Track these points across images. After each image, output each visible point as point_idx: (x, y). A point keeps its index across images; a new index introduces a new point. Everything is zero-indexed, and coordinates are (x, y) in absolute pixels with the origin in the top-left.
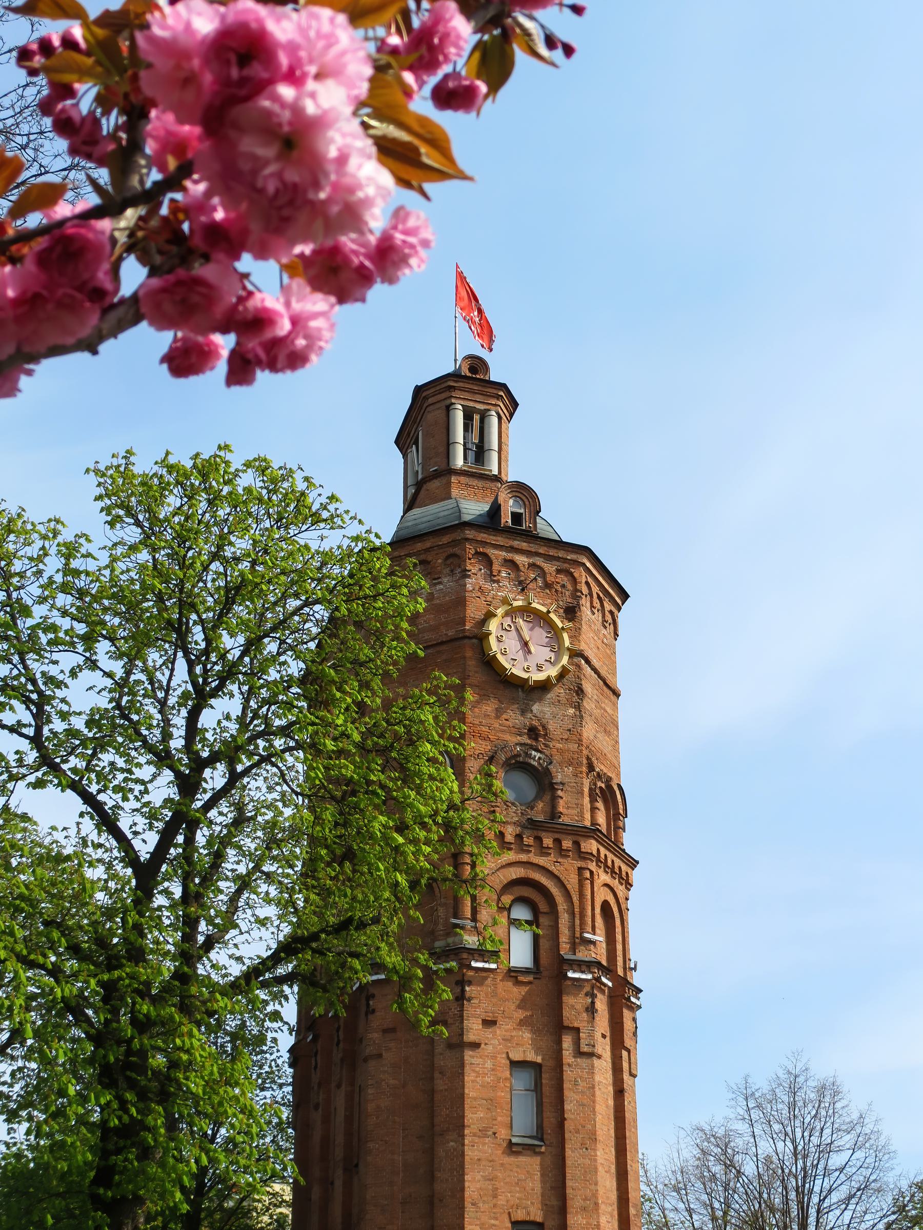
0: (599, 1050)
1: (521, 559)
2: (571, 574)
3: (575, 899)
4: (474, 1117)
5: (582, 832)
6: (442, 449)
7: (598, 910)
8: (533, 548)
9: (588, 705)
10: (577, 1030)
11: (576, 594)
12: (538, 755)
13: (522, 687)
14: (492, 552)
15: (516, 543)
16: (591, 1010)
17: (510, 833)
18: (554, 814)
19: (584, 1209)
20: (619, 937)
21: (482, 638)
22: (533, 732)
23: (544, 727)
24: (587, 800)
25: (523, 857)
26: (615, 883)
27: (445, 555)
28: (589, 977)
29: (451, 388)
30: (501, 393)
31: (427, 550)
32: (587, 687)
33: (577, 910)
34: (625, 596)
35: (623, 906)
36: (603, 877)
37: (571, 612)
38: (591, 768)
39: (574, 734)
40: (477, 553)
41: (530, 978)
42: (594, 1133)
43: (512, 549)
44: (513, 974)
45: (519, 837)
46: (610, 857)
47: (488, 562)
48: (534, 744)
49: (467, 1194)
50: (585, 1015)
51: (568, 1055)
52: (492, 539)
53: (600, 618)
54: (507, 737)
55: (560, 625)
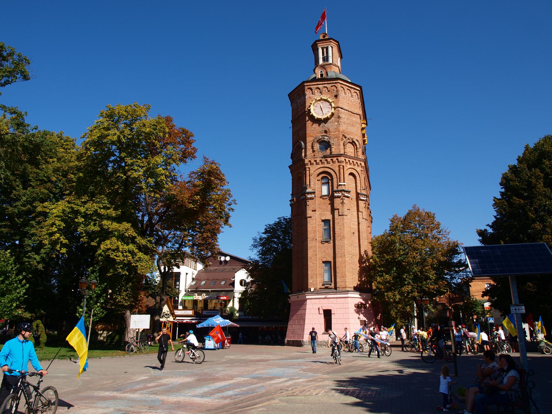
3: (338, 174)
4: (310, 236)
10: (338, 209)
11: (337, 91)
14: (312, 87)
15: (318, 83)
16: (343, 203)
18: (331, 153)
21: (309, 110)
22: (326, 132)
24: (342, 146)
25: (323, 166)
34: (360, 87)
35: (360, 173)
36: (349, 166)
37: (336, 96)
38: (345, 137)
39: (337, 129)
47: (311, 89)
49: (309, 255)
53: (350, 95)
54: (318, 135)
55: (331, 101)
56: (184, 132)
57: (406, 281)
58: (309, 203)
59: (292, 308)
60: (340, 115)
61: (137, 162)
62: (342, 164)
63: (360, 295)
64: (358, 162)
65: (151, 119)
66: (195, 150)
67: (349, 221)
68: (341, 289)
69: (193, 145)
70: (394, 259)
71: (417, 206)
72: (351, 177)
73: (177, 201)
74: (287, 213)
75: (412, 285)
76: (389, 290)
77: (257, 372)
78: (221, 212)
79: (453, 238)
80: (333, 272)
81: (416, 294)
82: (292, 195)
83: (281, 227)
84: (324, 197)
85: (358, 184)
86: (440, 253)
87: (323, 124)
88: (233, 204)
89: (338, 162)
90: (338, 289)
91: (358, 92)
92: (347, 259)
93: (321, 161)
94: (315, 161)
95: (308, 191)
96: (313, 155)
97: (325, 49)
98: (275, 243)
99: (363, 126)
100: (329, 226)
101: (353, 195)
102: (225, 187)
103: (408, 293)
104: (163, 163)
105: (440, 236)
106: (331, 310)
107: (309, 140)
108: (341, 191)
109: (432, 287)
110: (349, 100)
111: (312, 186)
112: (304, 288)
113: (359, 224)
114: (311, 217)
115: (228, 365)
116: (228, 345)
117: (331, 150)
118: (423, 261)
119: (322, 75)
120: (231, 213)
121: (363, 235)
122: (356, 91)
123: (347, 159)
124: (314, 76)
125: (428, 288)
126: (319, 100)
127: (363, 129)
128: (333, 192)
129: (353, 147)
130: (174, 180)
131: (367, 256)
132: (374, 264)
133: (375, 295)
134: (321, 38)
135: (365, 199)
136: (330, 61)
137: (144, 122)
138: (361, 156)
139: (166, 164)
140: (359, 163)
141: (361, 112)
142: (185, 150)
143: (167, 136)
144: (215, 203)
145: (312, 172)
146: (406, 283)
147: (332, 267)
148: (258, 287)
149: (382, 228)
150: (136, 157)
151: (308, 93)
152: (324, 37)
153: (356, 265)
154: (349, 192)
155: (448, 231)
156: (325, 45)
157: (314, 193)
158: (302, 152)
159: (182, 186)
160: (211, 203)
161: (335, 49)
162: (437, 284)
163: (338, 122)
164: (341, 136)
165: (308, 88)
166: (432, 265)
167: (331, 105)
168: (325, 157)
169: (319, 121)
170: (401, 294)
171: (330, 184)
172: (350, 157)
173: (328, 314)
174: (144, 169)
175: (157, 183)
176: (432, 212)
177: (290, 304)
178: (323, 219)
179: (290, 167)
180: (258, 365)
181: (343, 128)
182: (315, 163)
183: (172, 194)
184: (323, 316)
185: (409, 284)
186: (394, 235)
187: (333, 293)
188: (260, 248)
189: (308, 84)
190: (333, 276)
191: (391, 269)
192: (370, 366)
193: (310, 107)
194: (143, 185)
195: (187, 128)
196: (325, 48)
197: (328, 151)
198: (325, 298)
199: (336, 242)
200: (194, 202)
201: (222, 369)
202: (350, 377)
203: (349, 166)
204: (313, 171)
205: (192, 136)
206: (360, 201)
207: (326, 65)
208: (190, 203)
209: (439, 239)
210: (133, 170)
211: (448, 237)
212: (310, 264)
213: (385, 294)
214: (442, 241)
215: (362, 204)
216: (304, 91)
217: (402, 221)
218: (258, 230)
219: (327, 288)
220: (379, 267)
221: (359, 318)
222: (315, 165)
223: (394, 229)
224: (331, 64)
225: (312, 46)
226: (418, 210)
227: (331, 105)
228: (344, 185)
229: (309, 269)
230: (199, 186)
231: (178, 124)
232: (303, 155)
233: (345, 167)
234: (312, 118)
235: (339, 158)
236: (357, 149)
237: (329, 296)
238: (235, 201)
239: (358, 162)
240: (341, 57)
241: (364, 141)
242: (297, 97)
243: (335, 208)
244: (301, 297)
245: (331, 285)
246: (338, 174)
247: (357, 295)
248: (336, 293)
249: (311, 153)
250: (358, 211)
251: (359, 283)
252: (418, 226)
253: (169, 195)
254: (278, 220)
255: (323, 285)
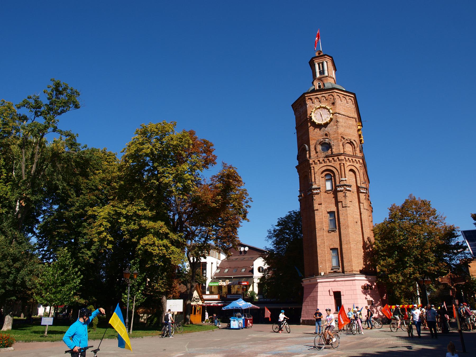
1: (318, 96)
3: (339, 171)
4: (318, 226)
14: (311, 97)
15: (317, 93)
16: (345, 196)
18: (332, 153)
19: (347, 243)
21: (311, 118)
22: (326, 135)
24: (341, 147)
25: (325, 164)
33: (340, 173)
34: (354, 94)
35: (359, 169)
36: (349, 164)
37: (333, 104)
38: (344, 139)
39: (336, 132)
42: (348, 225)
44: (326, 192)
47: (311, 99)
50: (343, 198)
51: (340, 208)
54: (320, 138)
55: (329, 108)
56: (205, 142)
57: (407, 263)
58: (315, 197)
59: (305, 291)
60: (338, 120)
61: (167, 170)
62: (343, 162)
63: (366, 277)
64: (356, 159)
65: (177, 133)
66: (215, 157)
67: (351, 212)
68: (348, 273)
69: (213, 153)
70: (395, 244)
71: (413, 196)
72: (351, 173)
73: (202, 201)
74: (296, 207)
75: (414, 267)
76: (392, 272)
77: (278, 349)
78: (239, 209)
79: (449, 222)
80: (340, 257)
81: (418, 275)
82: (300, 191)
83: (292, 220)
84: (328, 192)
85: (358, 179)
86: (438, 237)
87: (323, 129)
88: (250, 202)
89: (339, 160)
90: (345, 273)
91: (352, 99)
92: (352, 246)
93: (324, 160)
94: (319, 161)
95: (313, 187)
96: (316, 155)
97: (321, 64)
98: (287, 233)
99: (359, 127)
100: (334, 216)
101: (354, 189)
102: (242, 188)
103: (410, 275)
104: (189, 170)
105: (437, 222)
106: (340, 292)
107: (312, 143)
108: (343, 186)
109: (432, 268)
110: (345, 106)
111: (317, 182)
112: (315, 273)
113: (361, 214)
114: (317, 210)
115: (251, 342)
116: (251, 325)
117: (331, 150)
118: (422, 246)
119: (319, 87)
120: (248, 210)
121: (366, 224)
122: (350, 98)
123: (347, 158)
124: (313, 88)
125: (429, 269)
126: (319, 108)
127: (359, 130)
128: (336, 187)
129: (351, 146)
130: (198, 183)
131: (370, 242)
132: (377, 249)
133: (380, 277)
134: (317, 55)
135: (365, 191)
136: (326, 74)
137: (171, 135)
138: (359, 154)
139: (192, 170)
141: (356, 116)
142: (207, 158)
143: (191, 147)
144: (234, 201)
145: (316, 170)
146: (408, 265)
147: (339, 253)
148: (274, 273)
149: (382, 216)
150: (166, 166)
151: (309, 103)
152: (319, 54)
153: (361, 250)
154: (350, 186)
155: (443, 217)
156: (320, 60)
157: (319, 188)
158: (306, 154)
159: (206, 189)
160: (231, 202)
161: (330, 63)
162: (438, 265)
163: (337, 126)
164: (340, 138)
165: (309, 99)
166: (431, 248)
167: (329, 111)
168: (327, 157)
169: (320, 126)
170: (404, 275)
171: (333, 180)
172: (349, 156)
173: (337, 295)
174: (174, 175)
175: (184, 187)
176: (428, 200)
177: (303, 287)
178: (329, 211)
179: (297, 167)
180: (278, 342)
181: (341, 130)
182: (318, 162)
183: (197, 196)
184: (333, 297)
185: (410, 266)
186: (394, 222)
187: (341, 276)
188: (275, 238)
189: (308, 95)
190: (340, 262)
191: (393, 253)
192: (380, 342)
193: (311, 114)
194: (173, 189)
195: (207, 139)
196: (320, 63)
197: (329, 151)
198: (334, 281)
199: (342, 231)
200: (216, 201)
201: (247, 346)
202: (362, 353)
203: (349, 164)
204: (317, 170)
205: (212, 145)
206: (360, 194)
207: (323, 77)
208: (213, 202)
209: (436, 224)
210: (164, 176)
211: (445, 222)
212: (319, 251)
213: (389, 276)
214: (439, 226)
215: (362, 196)
216: (305, 101)
217: (400, 210)
218: (272, 223)
219: (335, 272)
220: (382, 251)
221: (366, 298)
222: (318, 165)
223: (393, 217)
224: (327, 76)
225: (309, 63)
226: (415, 199)
227: (329, 111)
228: (346, 180)
229: (319, 256)
230: (220, 188)
231: (200, 136)
232: (308, 156)
233: (345, 164)
234: (313, 124)
235: (339, 157)
236: (354, 148)
237: (337, 279)
238: (251, 198)
239: (356, 159)
240: (335, 70)
241: (361, 141)
242: (300, 107)
243: (339, 201)
244: (312, 281)
245: (339, 269)
246: (339, 171)
247: (363, 277)
248: (344, 276)
249: (315, 155)
250: (359, 202)
251: (364, 267)
252: (415, 213)
253: (195, 197)
254: (289, 214)
255: (332, 269)
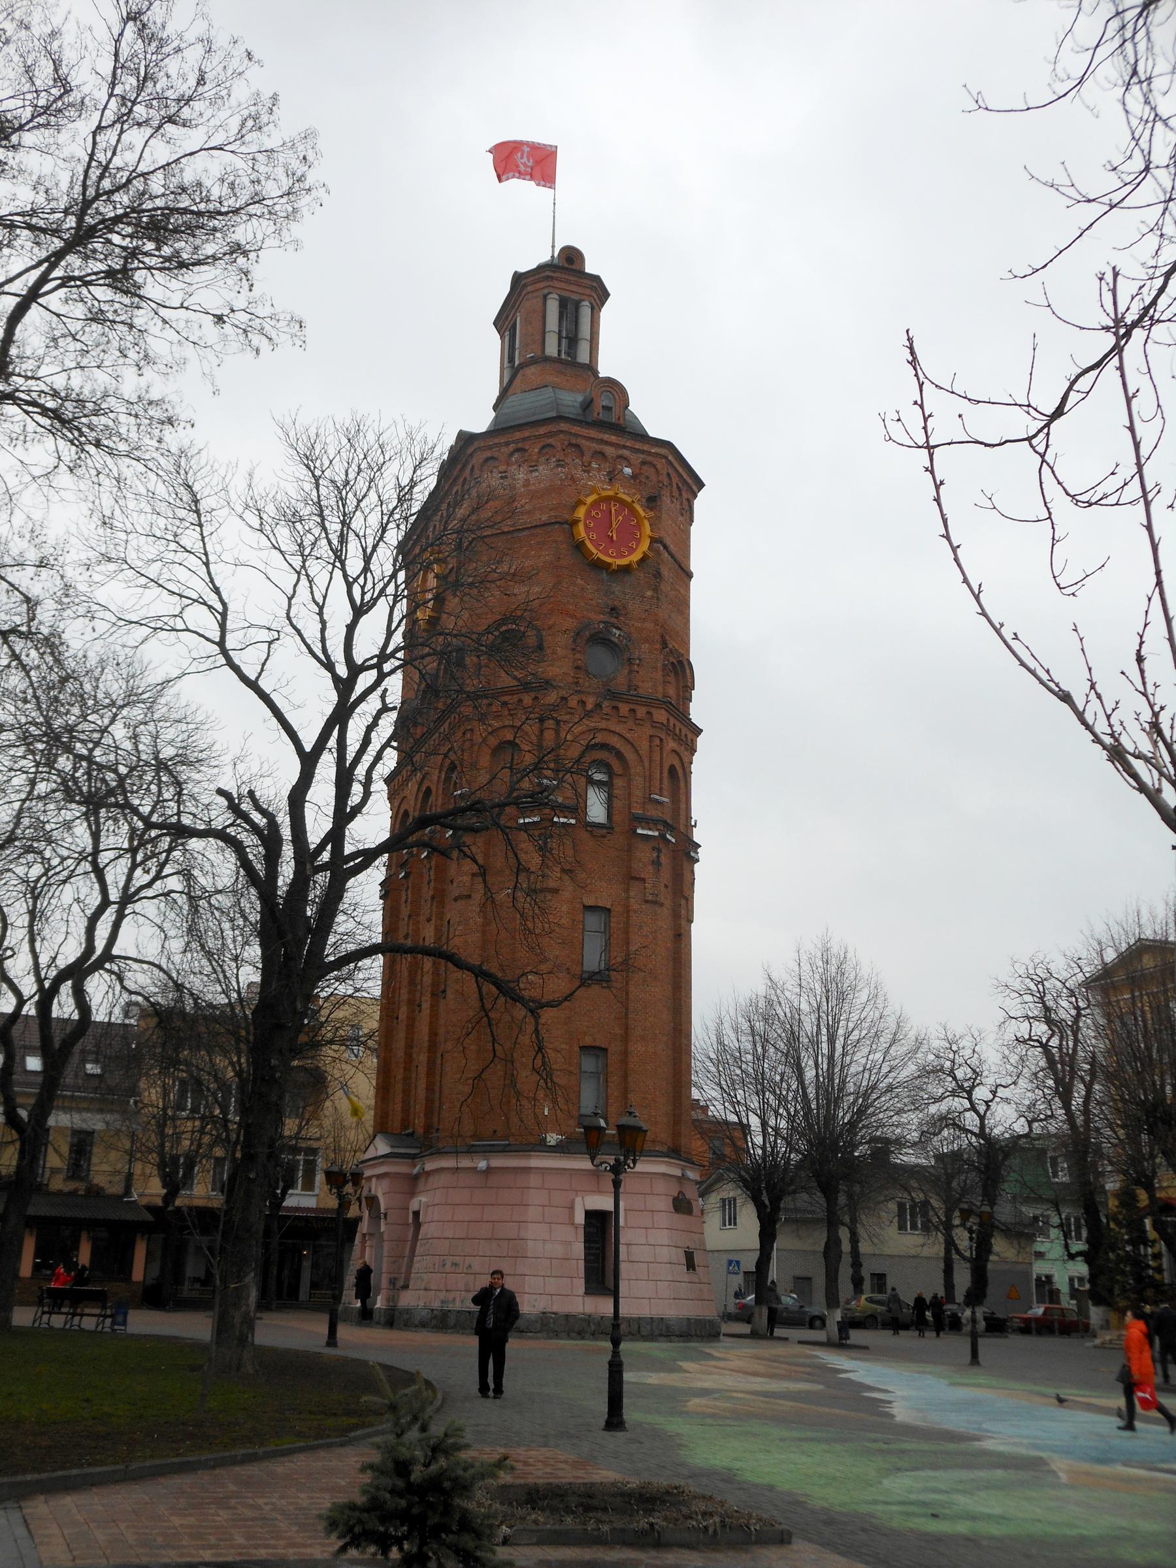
0: (662, 899)
1: (610, 451)
2: (654, 466)
5: (652, 703)
6: (538, 337)
7: (666, 774)
8: (621, 441)
9: (665, 587)
12: (618, 632)
13: (607, 569)
15: (606, 437)
16: (657, 863)
17: (590, 702)
20: (683, 798)
23: (625, 608)
26: (682, 750)
27: (539, 446)
28: (656, 834)
29: (548, 277)
30: (595, 284)
31: (524, 439)
32: (665, 572)
36: (671, 744)
37: (652, 501)
40: (570, 444)
41: (605, 831)
43: (602, 442)
45: (598, 706)
46: (678, 725)
48: (613, 620)
50: (650, 867)
51: (634, 904)
52: (584, 431)
54: (592, 615)
55: (642, 514)
96: (570, 680)
123: (672, 721)
140: (690, 735)
163: (656, 590)
165: (570, 444)
178: (589, 902)
184: (581, 1232)
246: (647, 764)
